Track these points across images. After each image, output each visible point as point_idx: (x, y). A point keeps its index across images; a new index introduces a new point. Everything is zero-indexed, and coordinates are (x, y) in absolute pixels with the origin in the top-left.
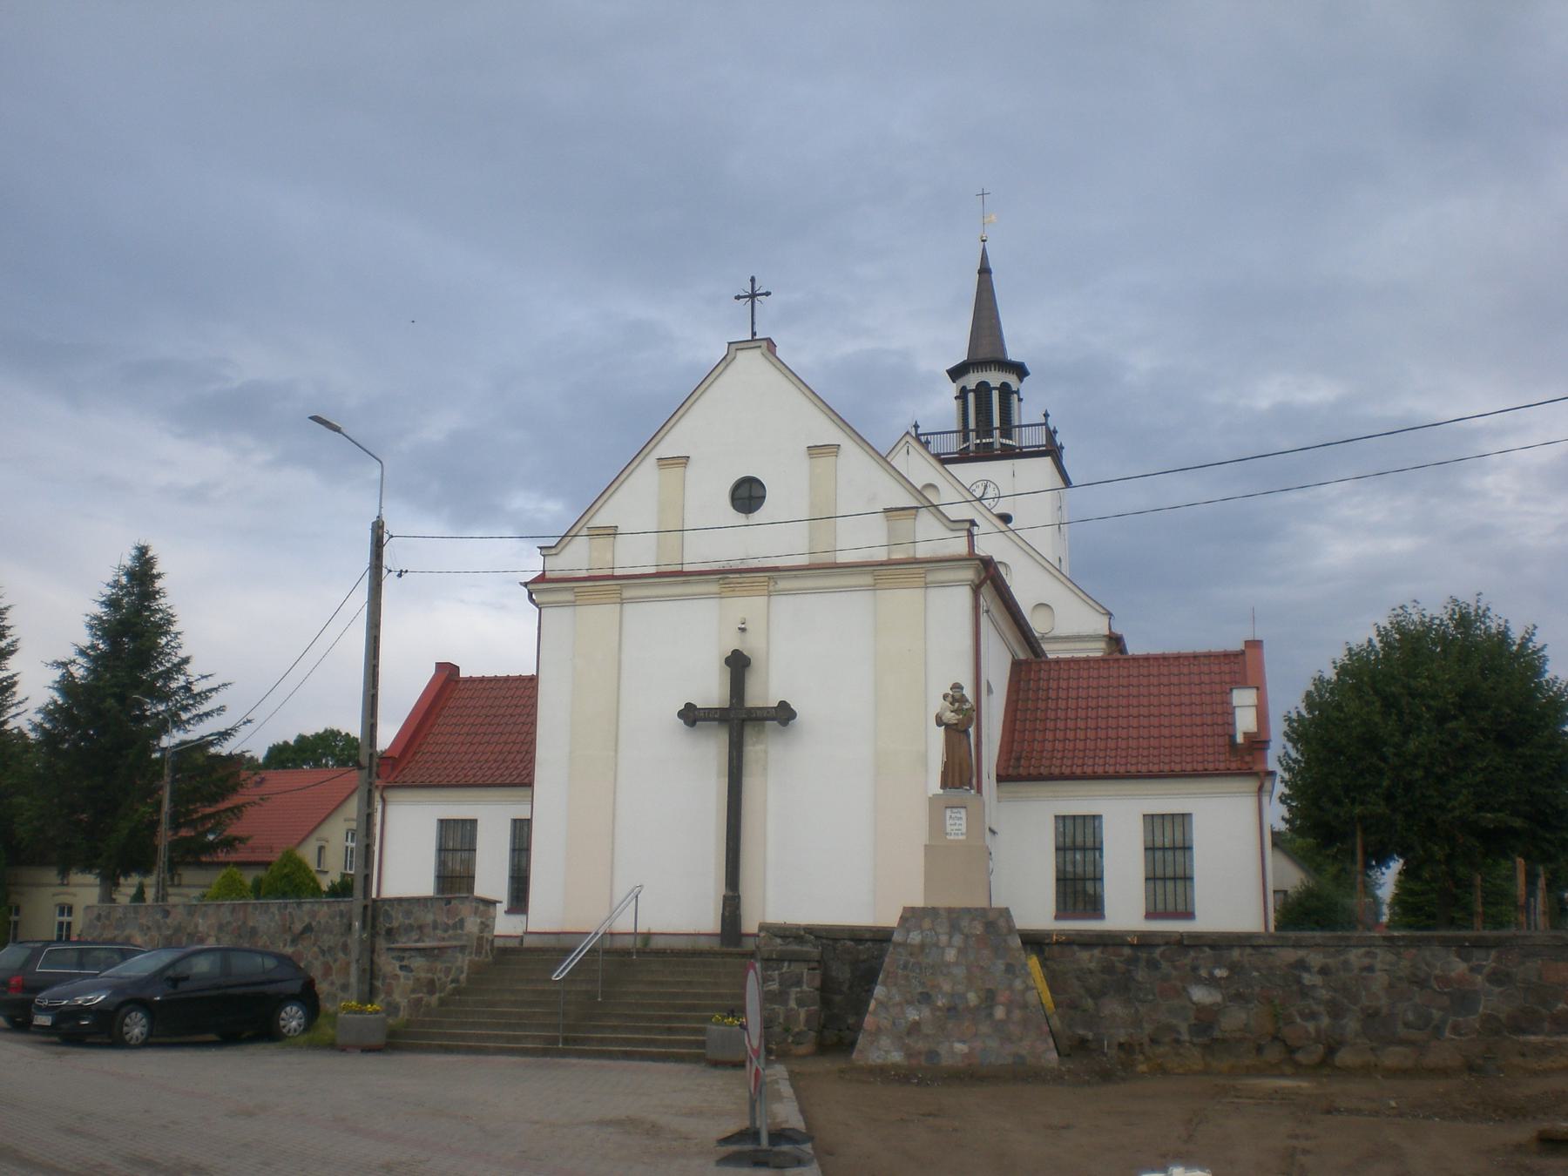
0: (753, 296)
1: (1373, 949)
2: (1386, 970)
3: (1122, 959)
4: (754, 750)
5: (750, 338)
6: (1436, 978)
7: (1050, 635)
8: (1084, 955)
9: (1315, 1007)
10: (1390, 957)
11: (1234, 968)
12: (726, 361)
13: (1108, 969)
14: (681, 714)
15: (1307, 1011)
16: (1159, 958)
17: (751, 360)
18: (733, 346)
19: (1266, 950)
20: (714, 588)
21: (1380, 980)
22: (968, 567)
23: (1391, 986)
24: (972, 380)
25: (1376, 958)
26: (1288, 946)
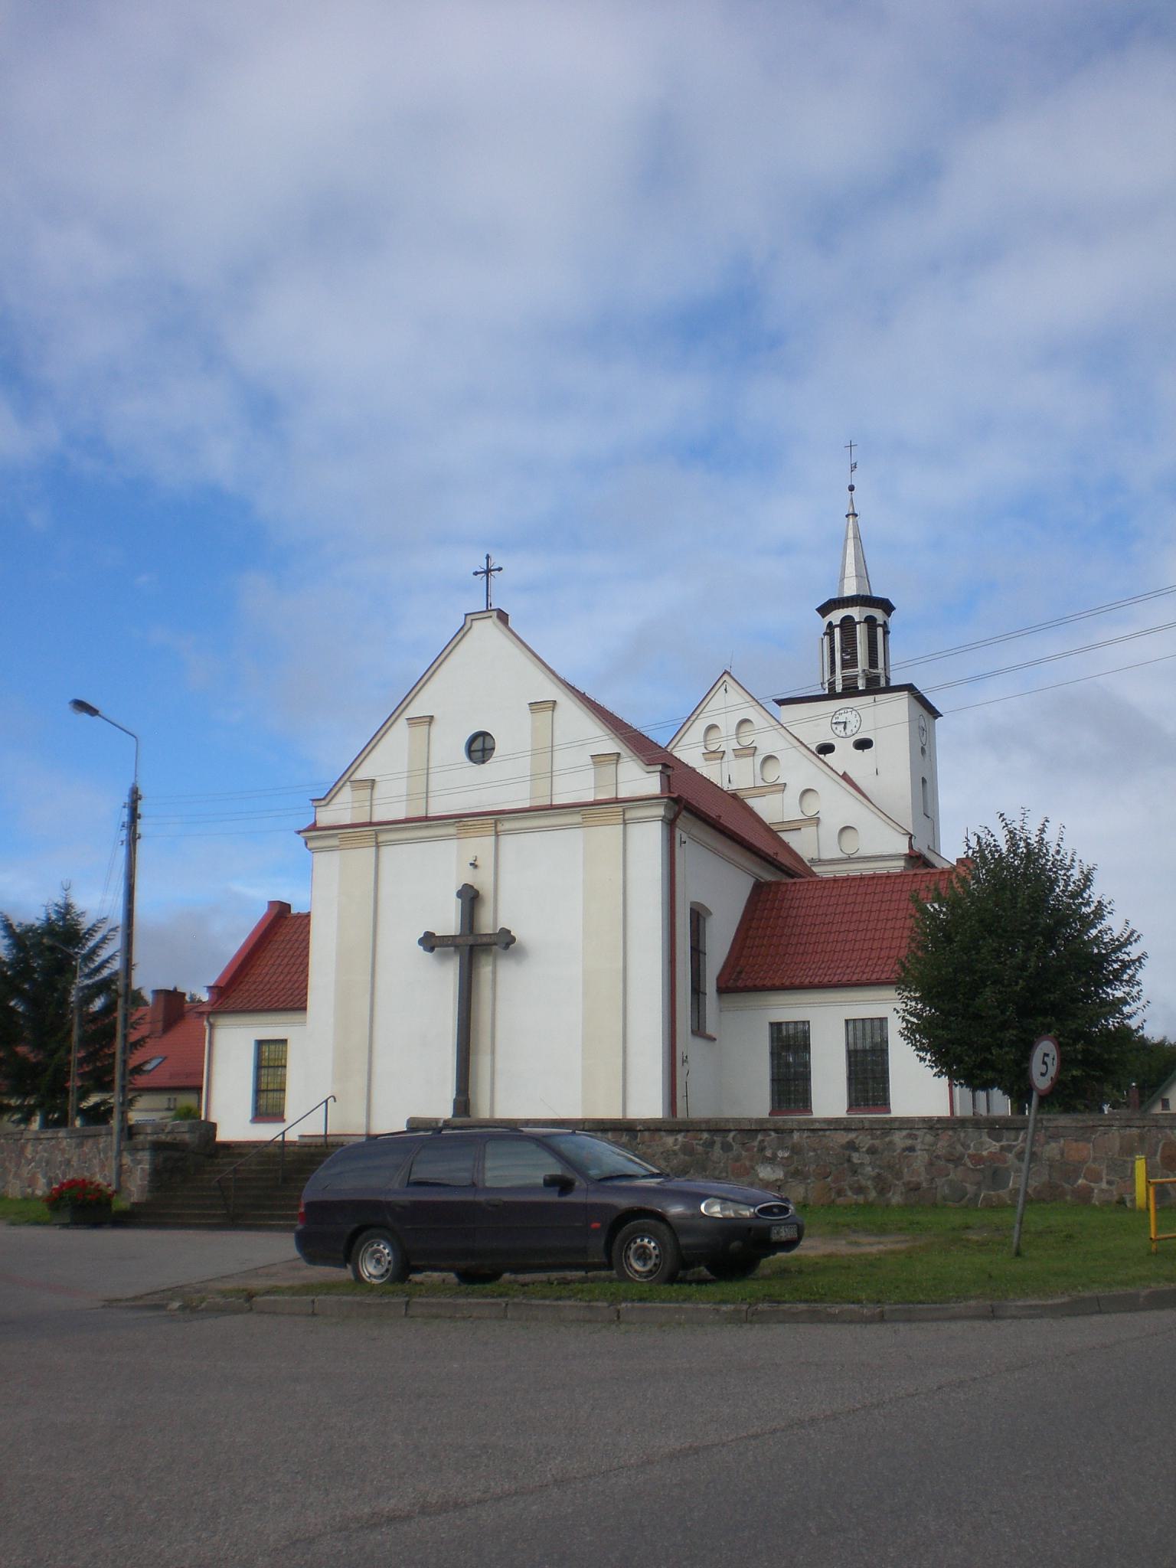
0: (488, 572)
1: (914, 1132)
2: (925, 1150)
3: (702, 1142)
4: (485, 970)
5: (485, 609)
6: (969, 1156)
7: (855, 856)
8: (669, 1140)
9: (863, 1182)
10: (929, 1138)
11: (796, 1150)
12: (462, 632)
13: (687, 1150)
14: (421, 942)
15: (856, 1185)
16: (731, 1141)
17: (487, 630)
18: (469, 618)
19: (821, 1133)
20: (452, 830)
21: (920, 1158)
22: (658, 805)
23: (931, 1164)
24: (836, 616)
25: (916, 1139)
26: (841, 1129)
